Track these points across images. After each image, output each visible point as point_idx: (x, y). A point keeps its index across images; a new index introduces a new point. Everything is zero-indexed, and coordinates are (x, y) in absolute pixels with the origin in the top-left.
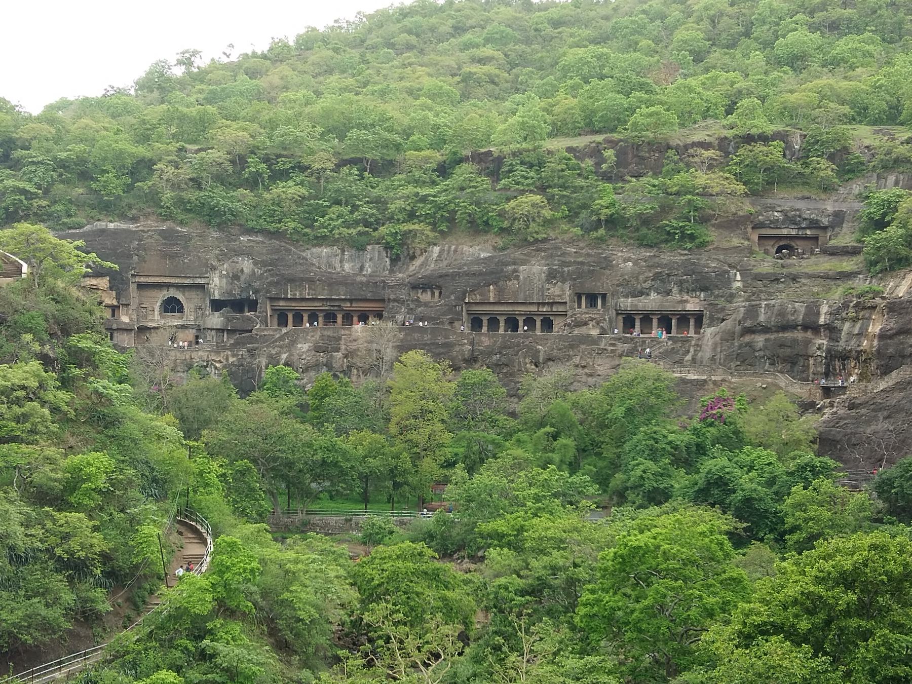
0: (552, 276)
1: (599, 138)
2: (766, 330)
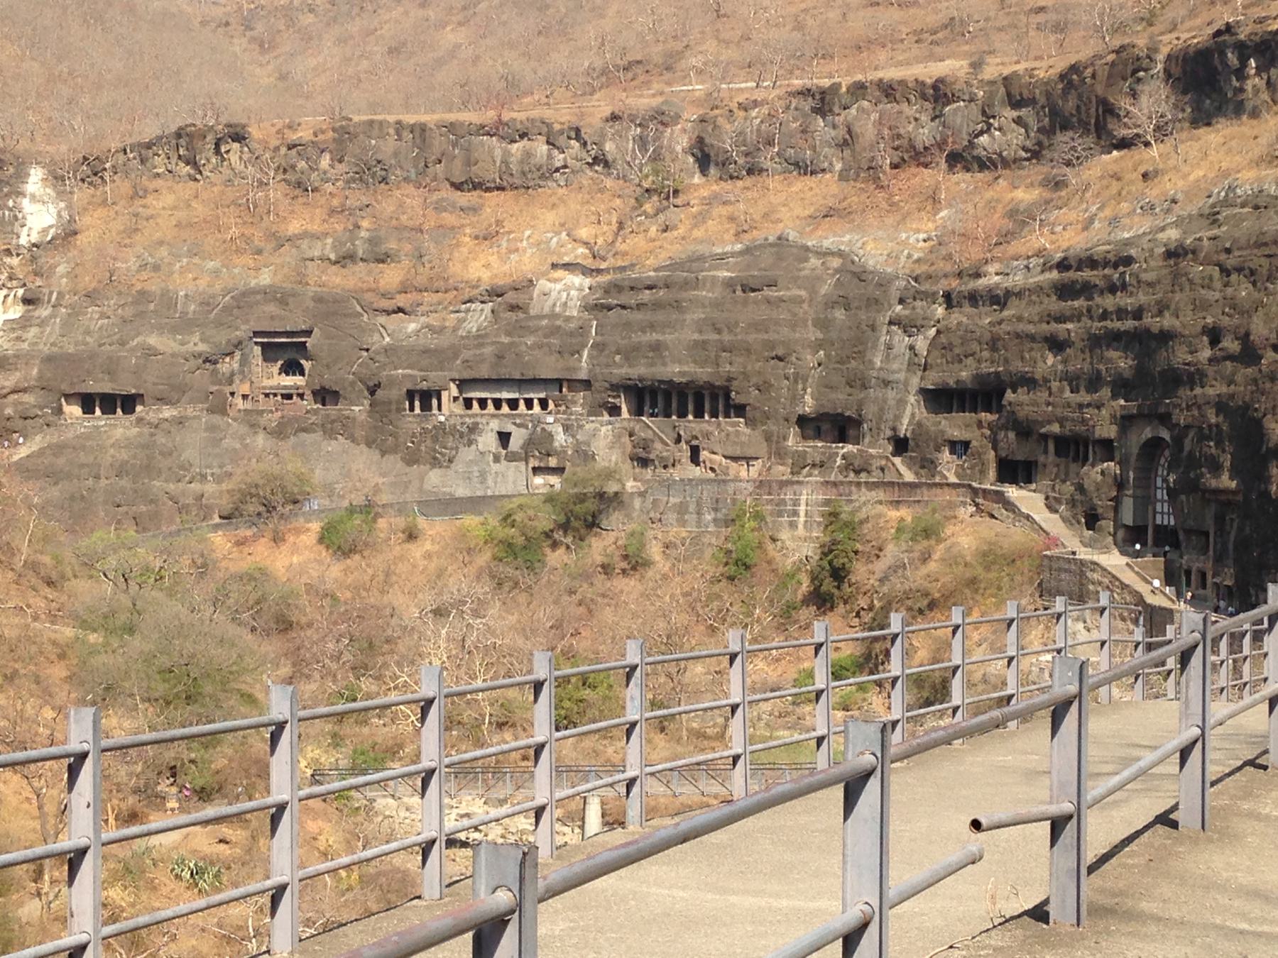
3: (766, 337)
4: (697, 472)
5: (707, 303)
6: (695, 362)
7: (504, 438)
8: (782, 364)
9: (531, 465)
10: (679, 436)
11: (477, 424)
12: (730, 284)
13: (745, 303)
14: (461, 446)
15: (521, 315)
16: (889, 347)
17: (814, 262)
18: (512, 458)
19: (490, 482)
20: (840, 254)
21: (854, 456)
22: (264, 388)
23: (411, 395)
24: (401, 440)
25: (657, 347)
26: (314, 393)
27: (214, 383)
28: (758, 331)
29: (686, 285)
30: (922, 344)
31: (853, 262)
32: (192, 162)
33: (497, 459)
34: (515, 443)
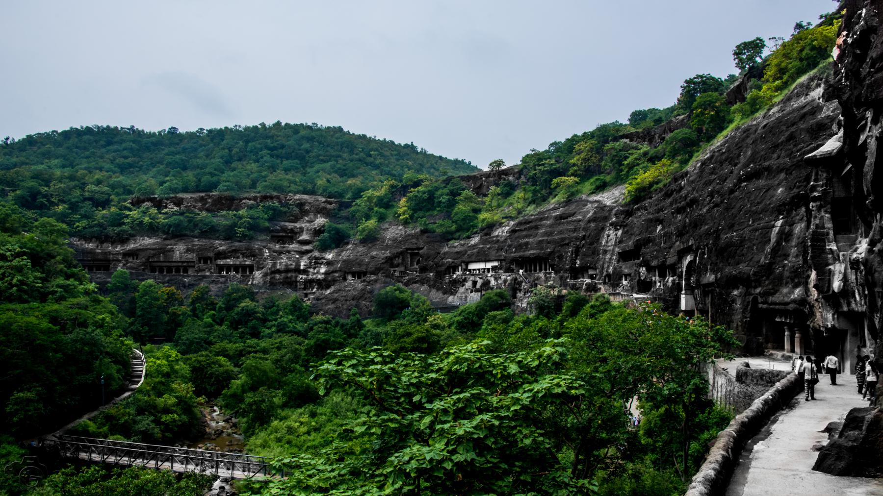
0: (188, 250)
1: (203, 194)
2: (279, 272)
3: (563, 236)
16: (609, 236)
17: (589, 205)
25: (527, 244)
30: (620, 233)
34: (478, 286)
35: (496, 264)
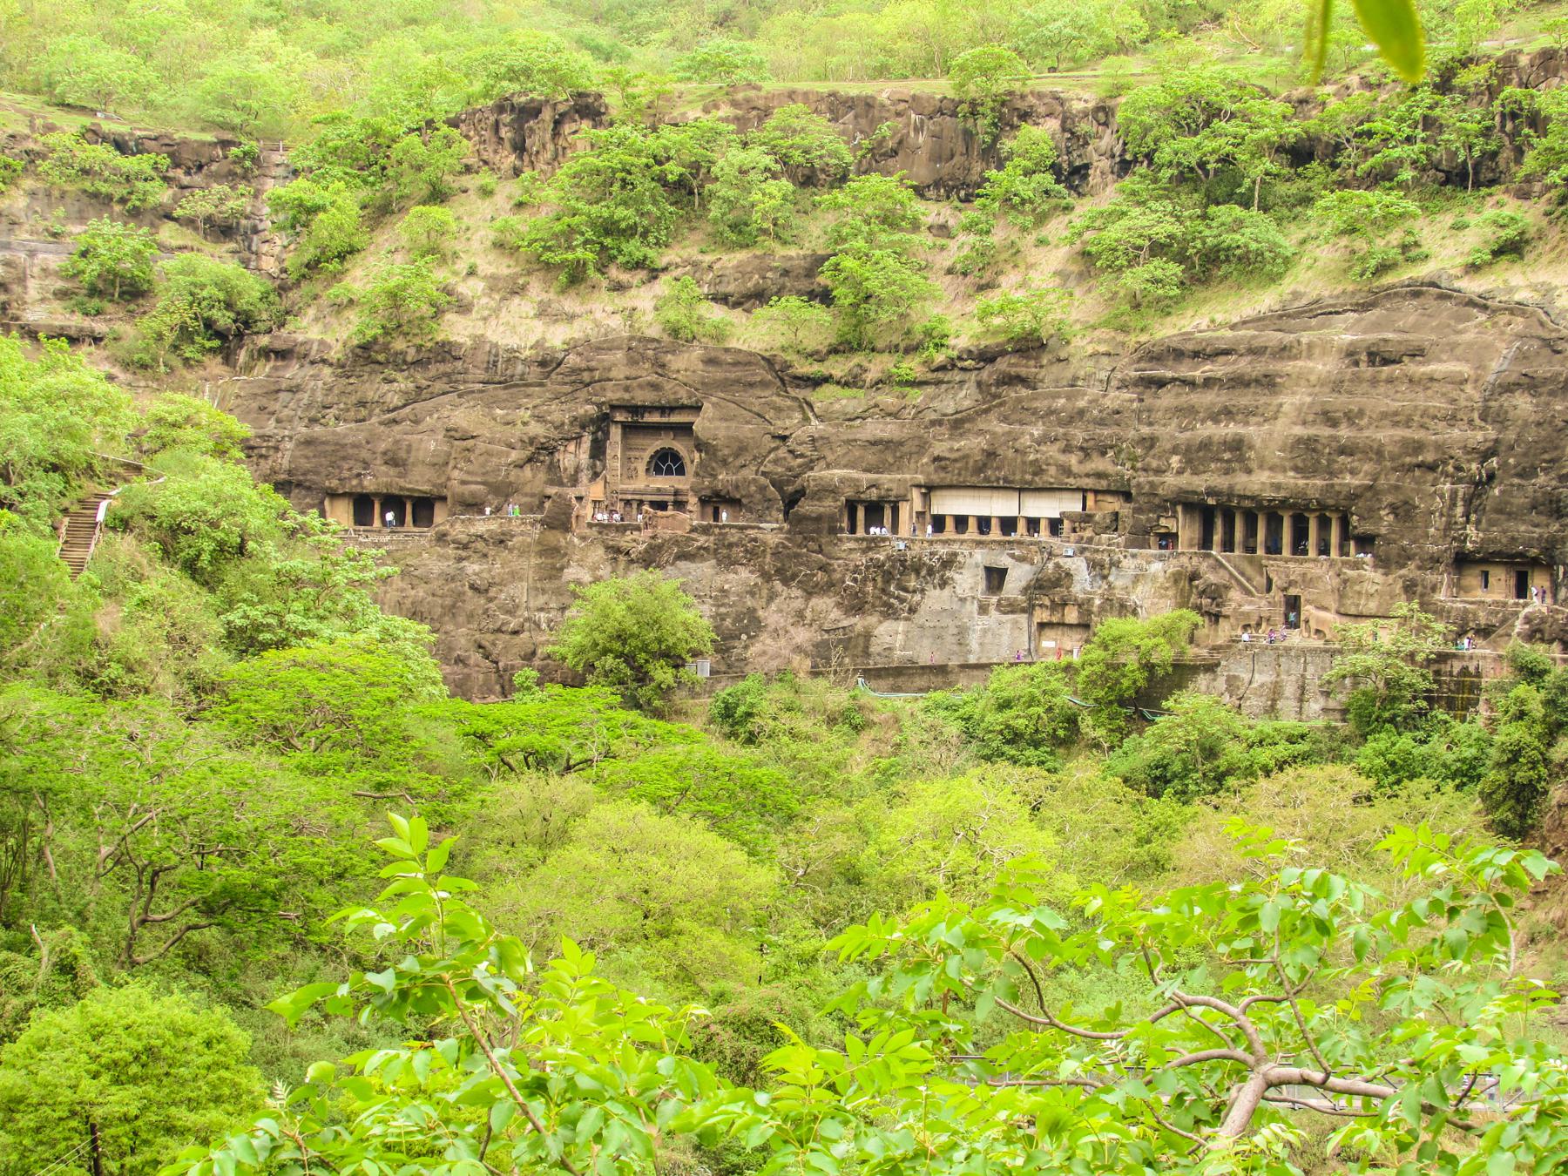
3: (1407, 433)
4: (1296, 638)
5: (1313, 378)
6: (1296, 469)
7: (995, 577)
8: (1430, 477)
9: (1036, 620)
10: (1270, 581)
11: (955, 554)
12: (1351, 354)
13: (1374, 382)
14: (929, 587)
15: (1024, 392)
18: (1010, 608)
19: (973, 642)
20: (1518, 309)
21: (1543, 620)
22: (624, 492)
23: (851, 506)
24: (837, 576)
25: (1237, 446)
26: (703, 502)
27: (551, 483)
28: (1396, 424)
29: (1283, 352)
31: (1542, 324)
32: (520, 148)
33: (983, 609)
35: (1073, 505)
